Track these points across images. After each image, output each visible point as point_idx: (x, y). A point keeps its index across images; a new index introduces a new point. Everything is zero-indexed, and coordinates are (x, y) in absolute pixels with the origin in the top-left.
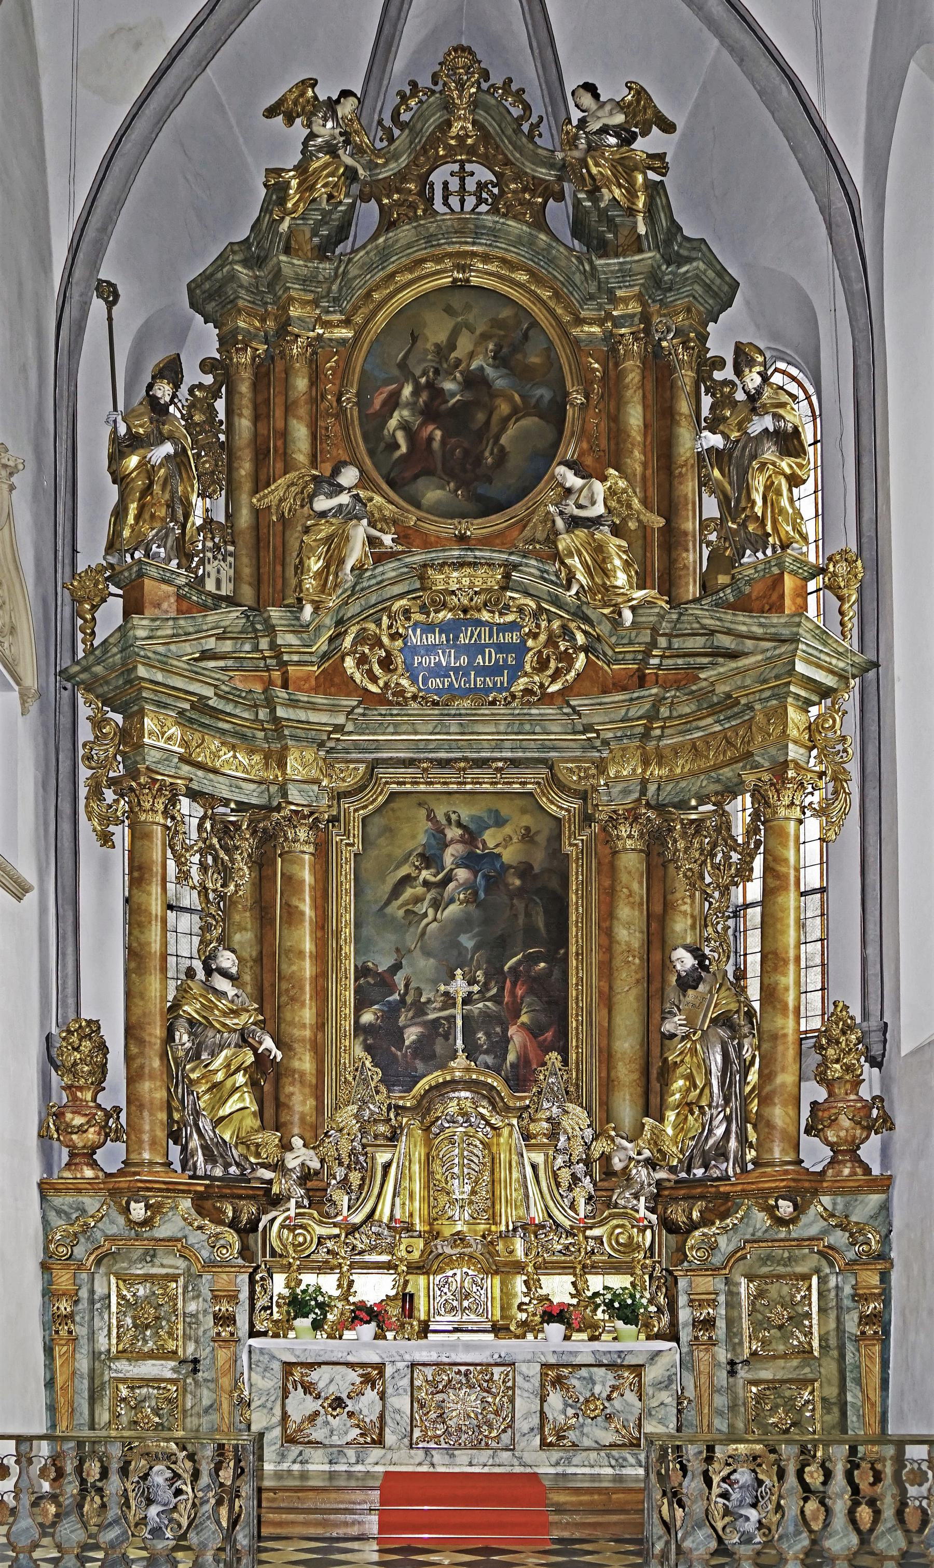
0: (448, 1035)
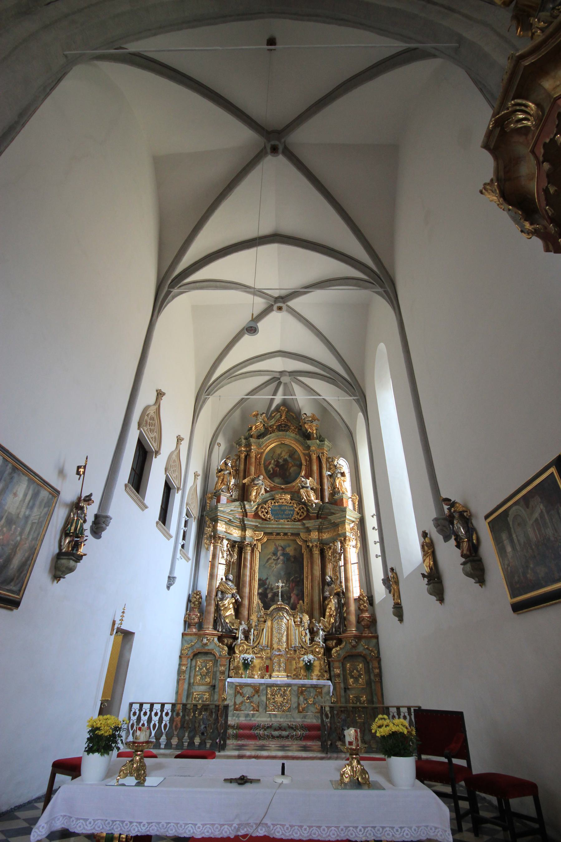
0: (278, 596)
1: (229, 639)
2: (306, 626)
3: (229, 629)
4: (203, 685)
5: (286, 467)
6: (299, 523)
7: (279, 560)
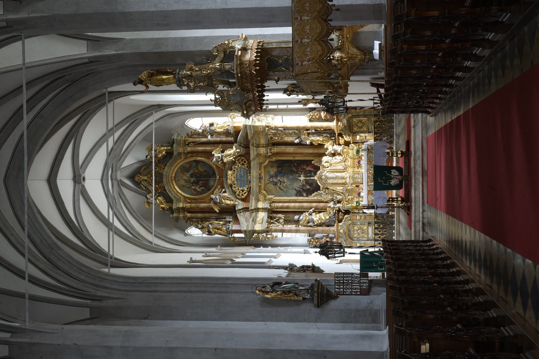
1: (340, 215)
2: (330, 158)
3: (333, 215)
5: (198, 175)
6: (252, 163)
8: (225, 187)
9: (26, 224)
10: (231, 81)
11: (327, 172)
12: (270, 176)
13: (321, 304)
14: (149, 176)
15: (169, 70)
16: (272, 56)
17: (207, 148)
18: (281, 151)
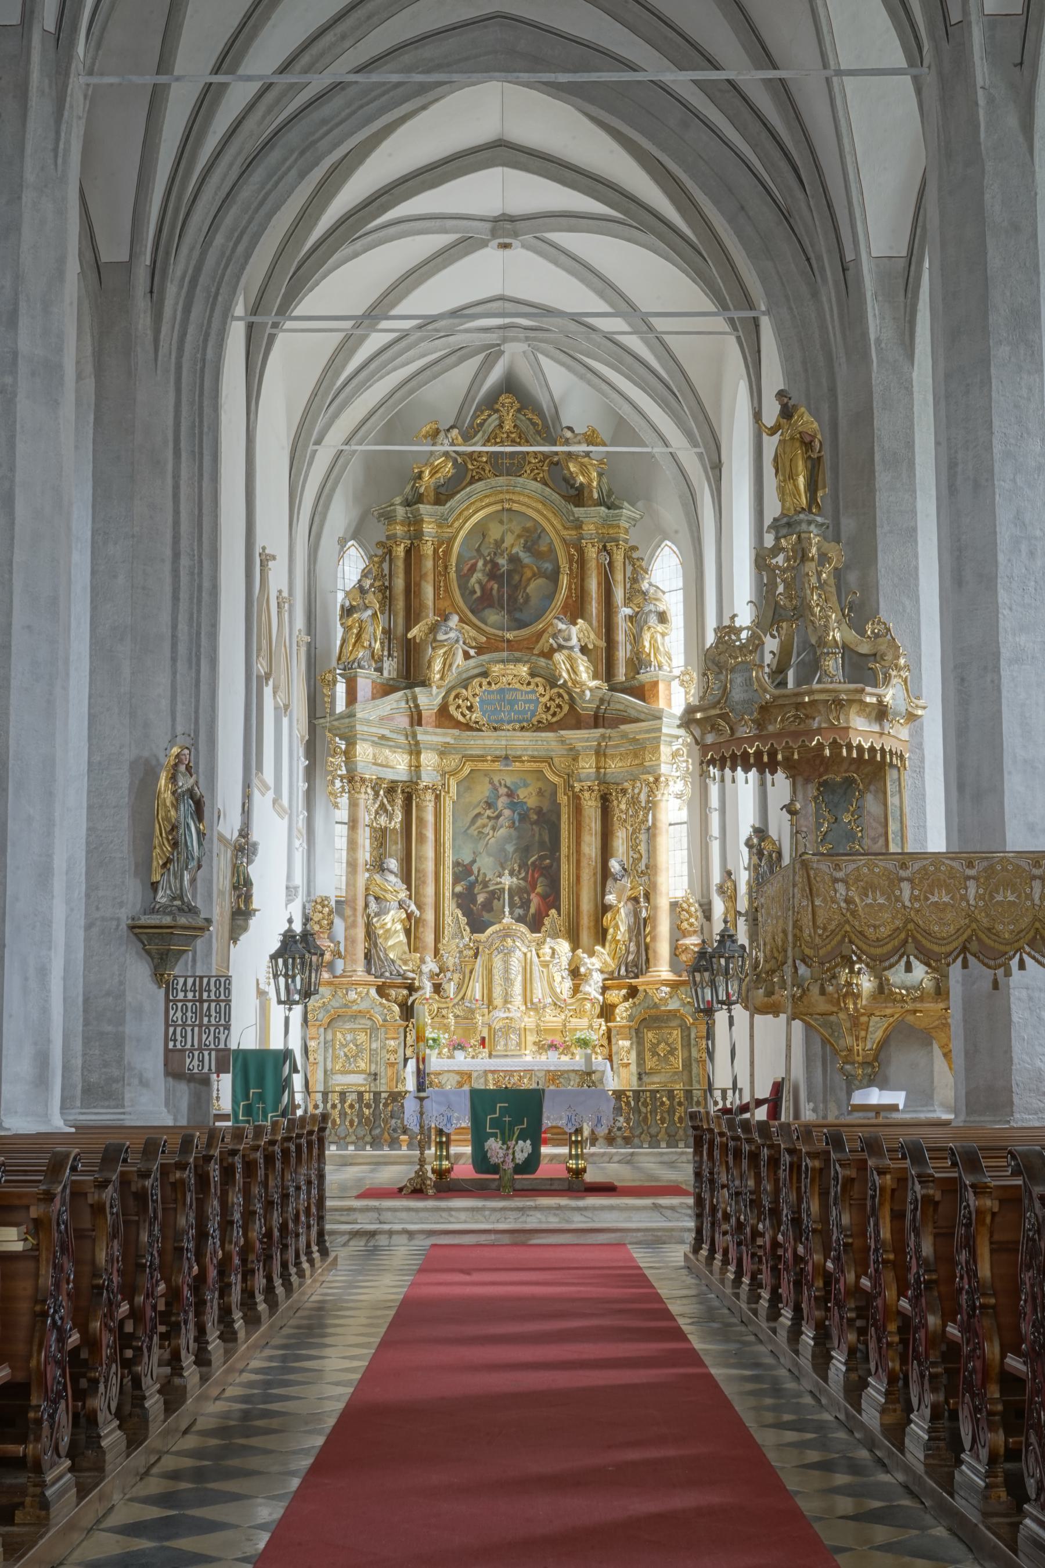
1: (400, 990)
4: (354, 1072)
5: (517, 578)
7: (501, 819)
8: (482, 657)
9: (375, 78)
10: (791, 674)
11: (525, 954)
12: (512, 787)
13: (136, 934)
14: (513, 436)
15: (820, 494)
16: (862, 794)
17: (594, 604)
18: (587, 820)
